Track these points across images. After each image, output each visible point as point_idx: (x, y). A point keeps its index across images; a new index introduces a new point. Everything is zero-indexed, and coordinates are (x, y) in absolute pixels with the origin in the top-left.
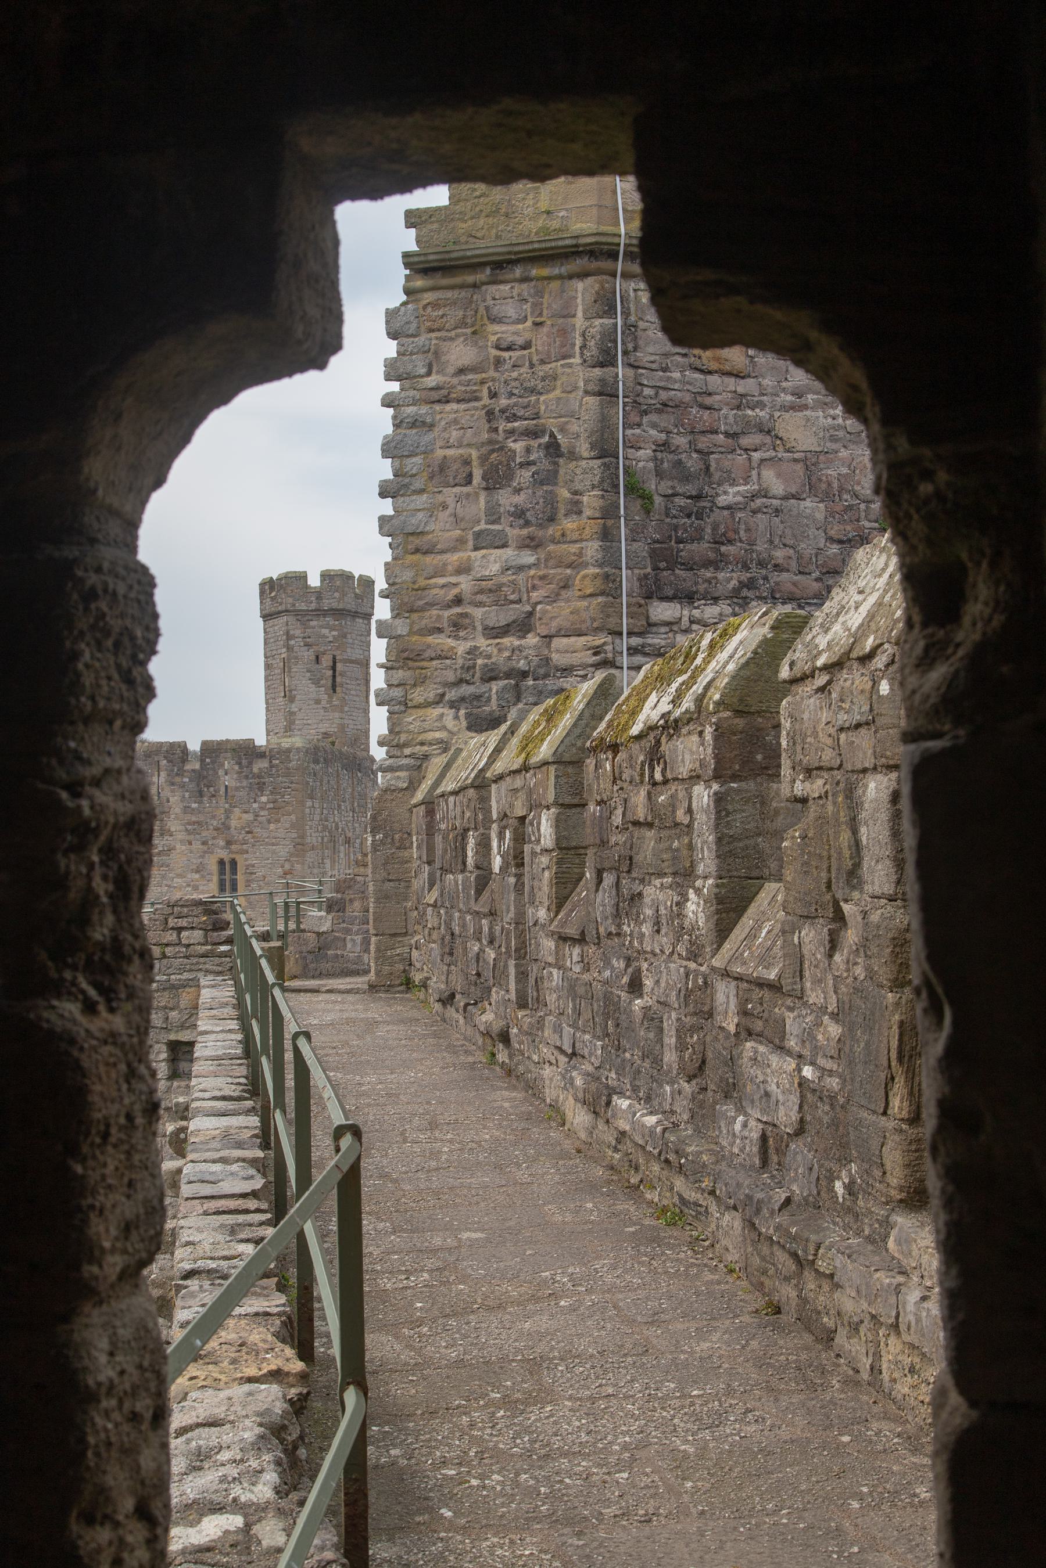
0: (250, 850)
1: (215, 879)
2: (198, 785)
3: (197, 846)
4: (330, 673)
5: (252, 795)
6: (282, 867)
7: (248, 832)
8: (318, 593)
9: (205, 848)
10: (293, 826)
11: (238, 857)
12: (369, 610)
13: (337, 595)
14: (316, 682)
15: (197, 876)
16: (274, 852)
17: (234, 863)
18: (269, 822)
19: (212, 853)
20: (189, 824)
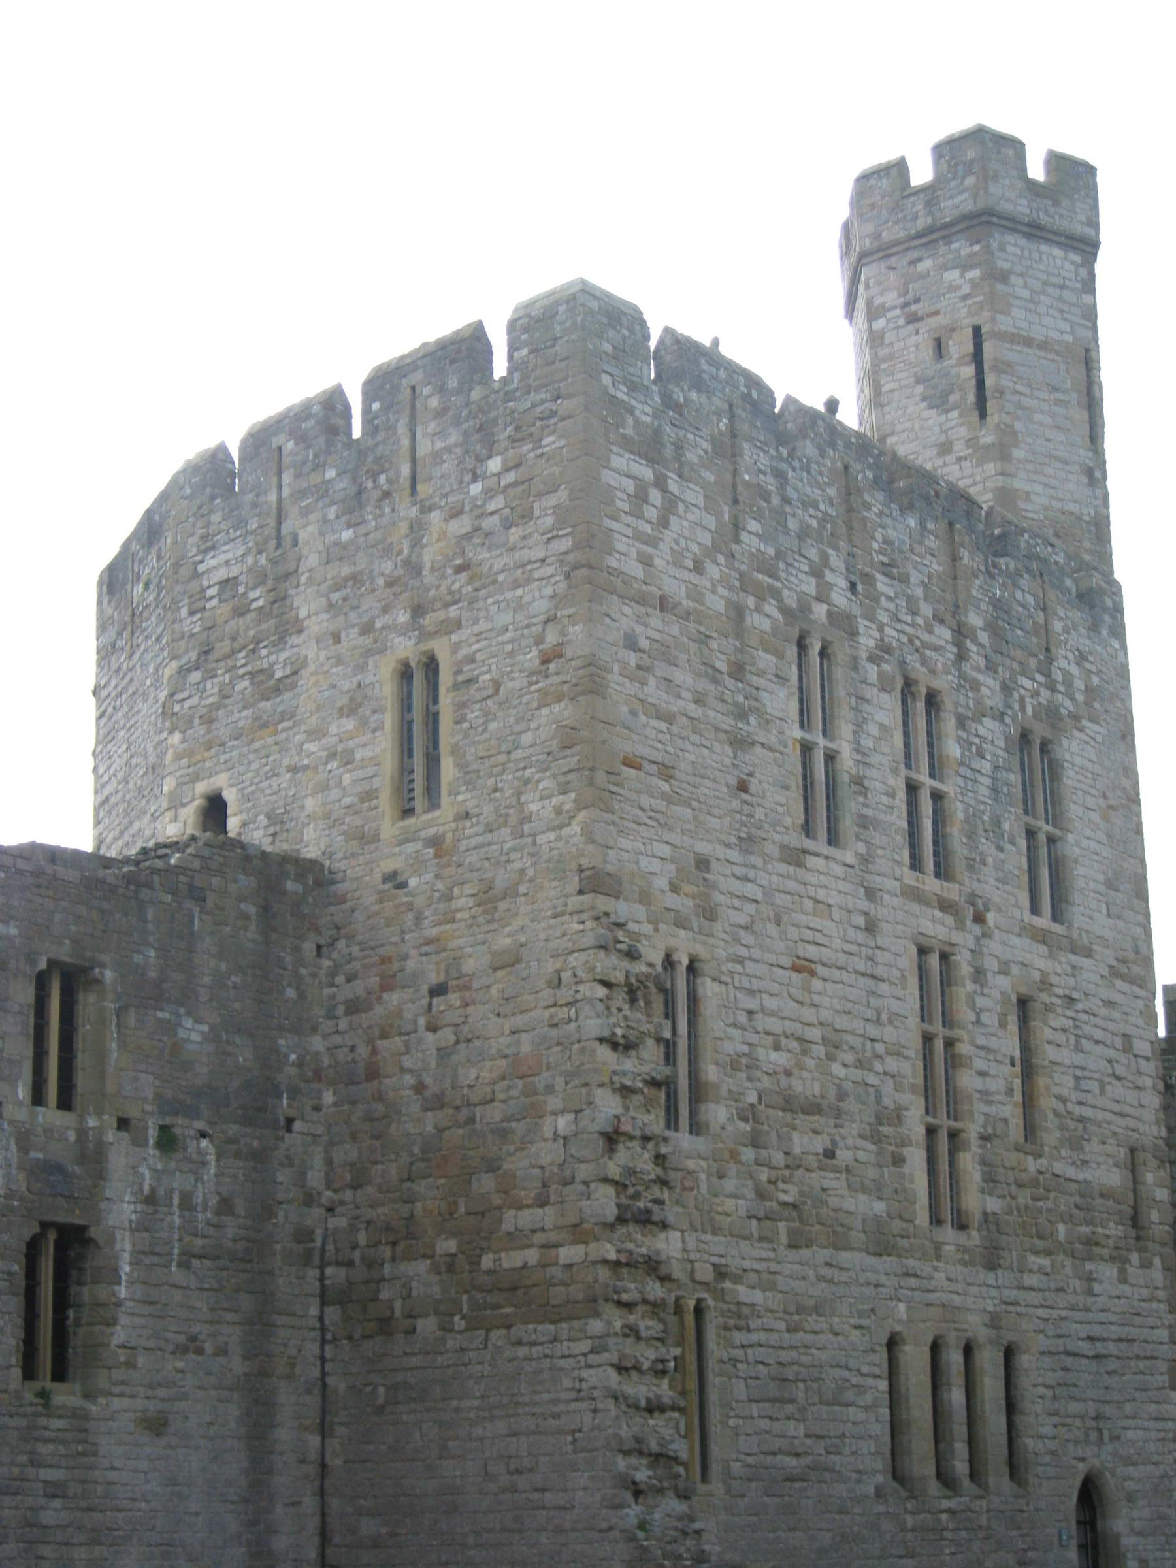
0: (466, 615)
1: (389, 720)
2: (354, 479)
3: (352, 638)
4: (969, 371)
5: (470, 462)
6: (539, 640)
7: (459, 570)
8: (929, 191)
9: (367, 641)
10: (562, 516)
11: (441, 648)
12: (1079, 229)
13: (970, 181)
14: (939, 401)
15: (350, 724)
16: (519, 606)
17: (431, 665)
18: (508, 525)
19: (382, 651)
20: (336, 588)
